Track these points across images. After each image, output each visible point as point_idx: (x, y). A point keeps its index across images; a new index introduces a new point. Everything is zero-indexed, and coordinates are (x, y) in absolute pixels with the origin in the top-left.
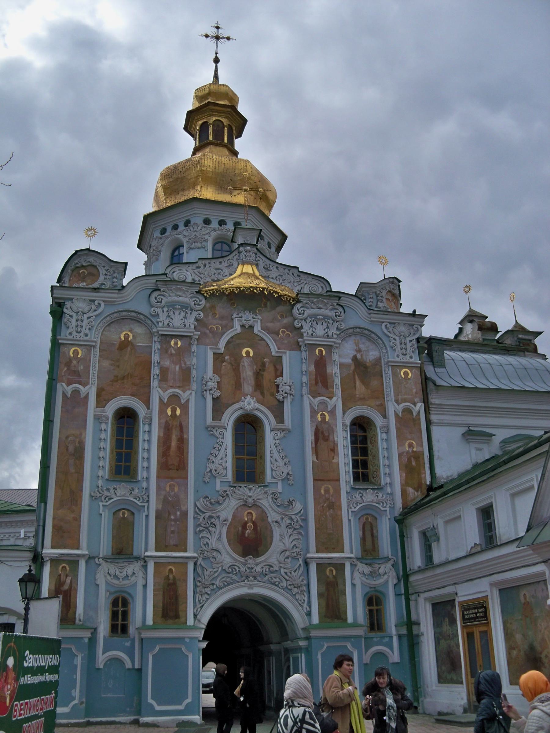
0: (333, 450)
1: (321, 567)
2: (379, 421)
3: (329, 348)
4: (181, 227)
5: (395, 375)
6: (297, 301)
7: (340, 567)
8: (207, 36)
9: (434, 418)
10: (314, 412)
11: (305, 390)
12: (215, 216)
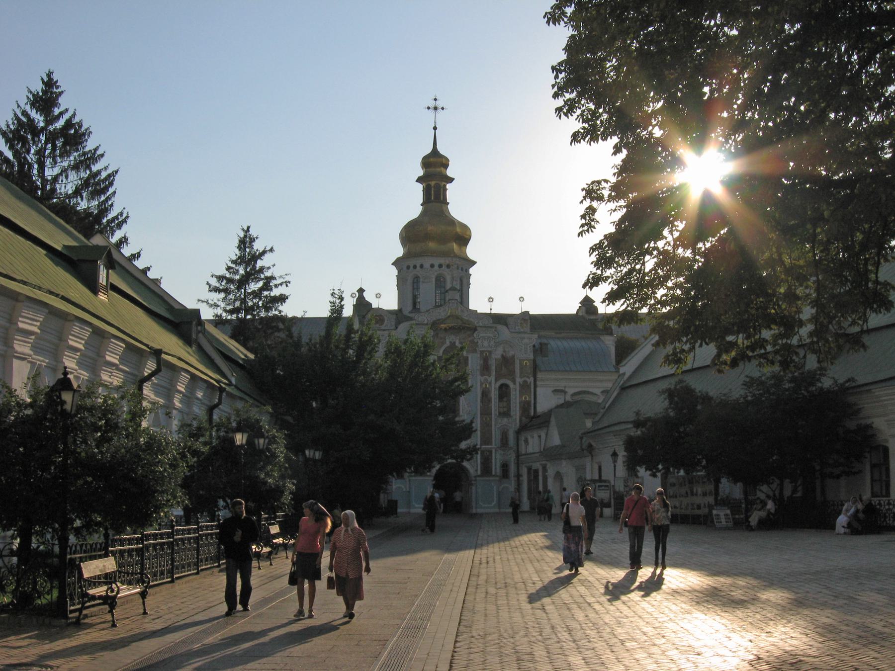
0: (490, 401)
1: (483, 452)
2: (511, 385)
3: (490, 352)
4: (418, 268)
5: (520, 364)
6: (475, 329)
7: (491, 452)
8: (429, 108)
9: (538, 383)
10: (482, 384)
11: (478, 373)
12: (437, 261)
